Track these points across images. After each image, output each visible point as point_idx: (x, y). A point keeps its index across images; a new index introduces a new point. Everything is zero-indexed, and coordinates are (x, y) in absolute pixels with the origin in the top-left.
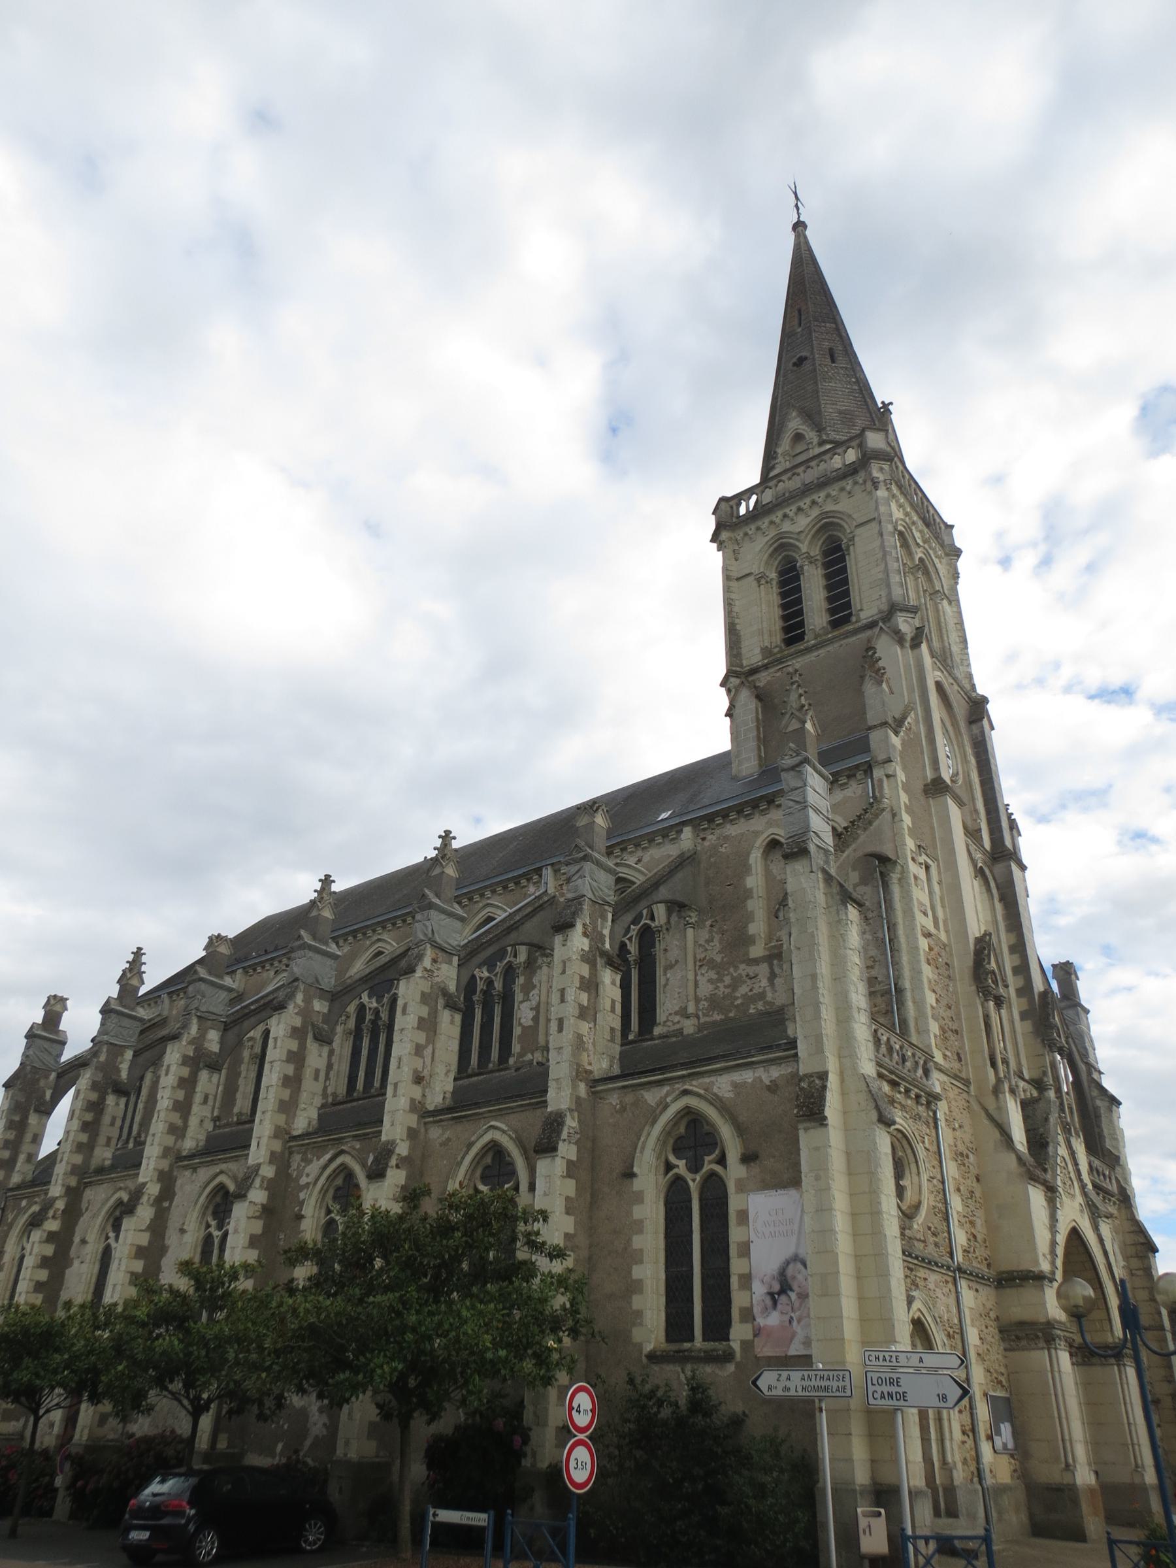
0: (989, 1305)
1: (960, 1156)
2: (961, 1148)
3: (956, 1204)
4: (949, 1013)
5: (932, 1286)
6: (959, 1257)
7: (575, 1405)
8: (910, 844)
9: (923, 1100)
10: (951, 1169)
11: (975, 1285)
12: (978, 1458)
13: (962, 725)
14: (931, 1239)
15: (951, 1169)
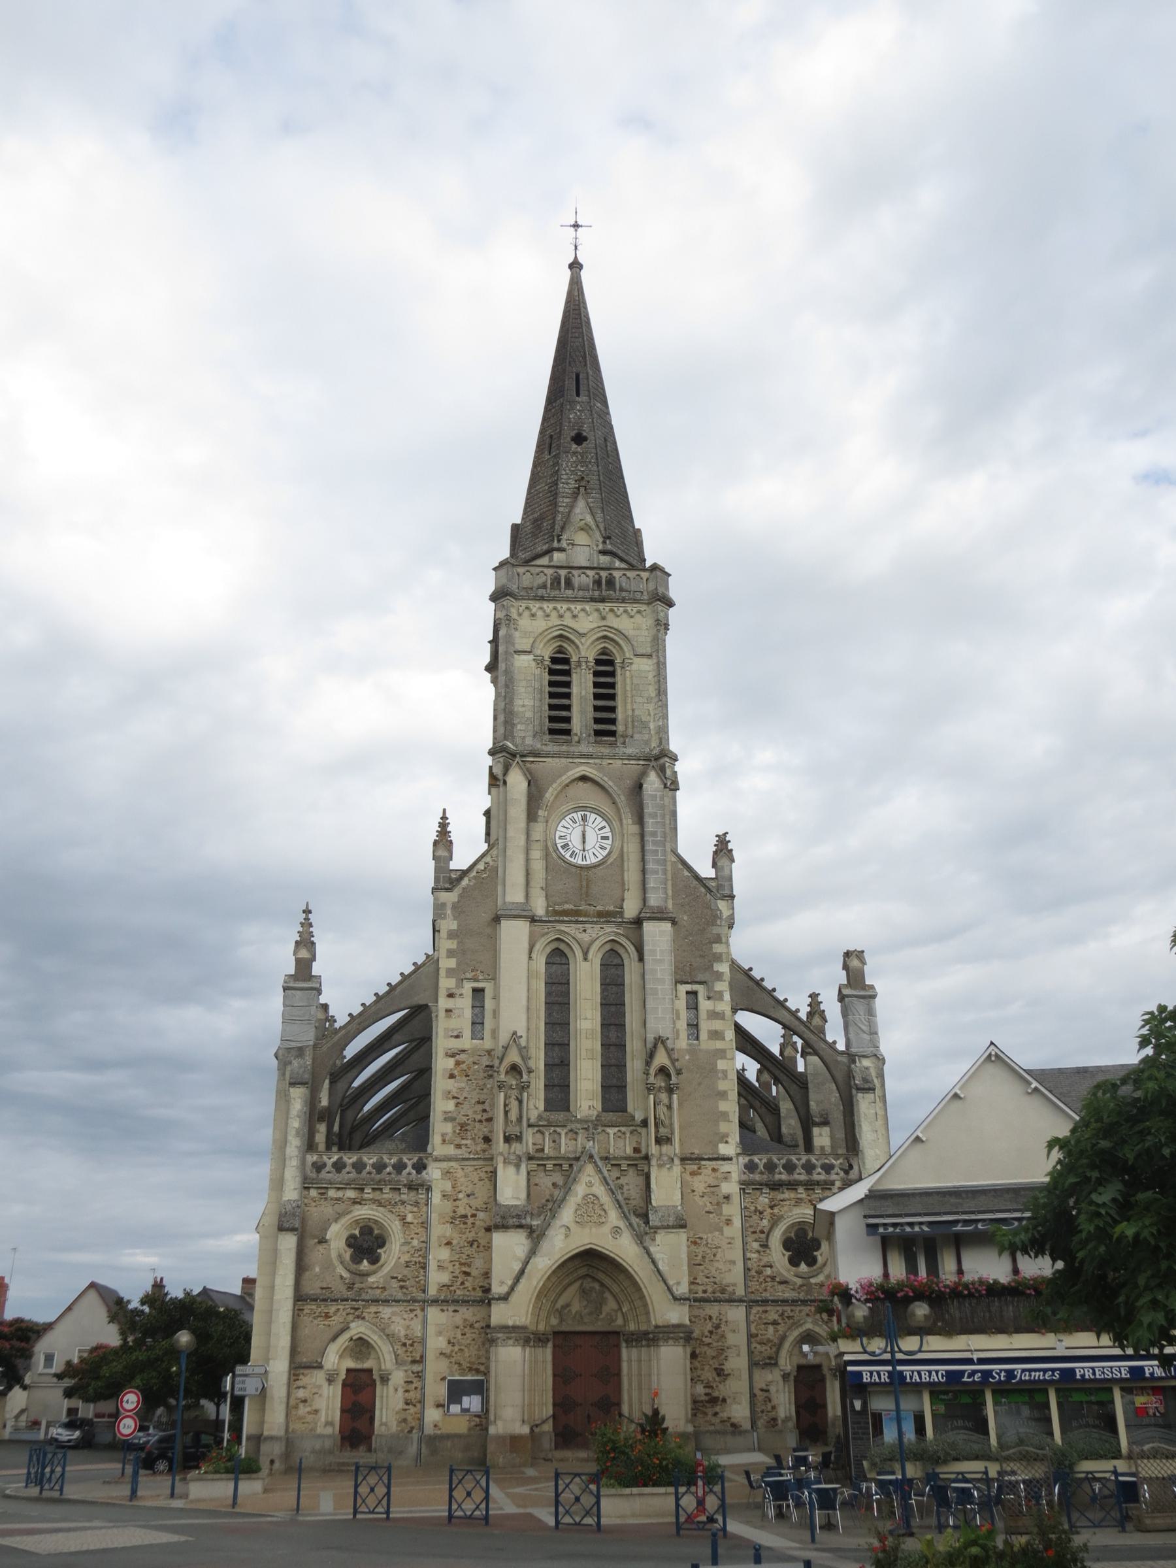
0: (472, 1319)
1: (459, 1219)
2: (461, 1211)
3: (439, 1254)
4: (480, 1107)
5: (386, 1316)
6: (432, 1291)
7: (125, 1399)
8: (446, 983)
9: (405, 1190)
10: (439, 1230)
11: (451, 1308)
12: (421, 1419)
13: (622, 800)
14: (395, 1284)
15: (439, 1230)
